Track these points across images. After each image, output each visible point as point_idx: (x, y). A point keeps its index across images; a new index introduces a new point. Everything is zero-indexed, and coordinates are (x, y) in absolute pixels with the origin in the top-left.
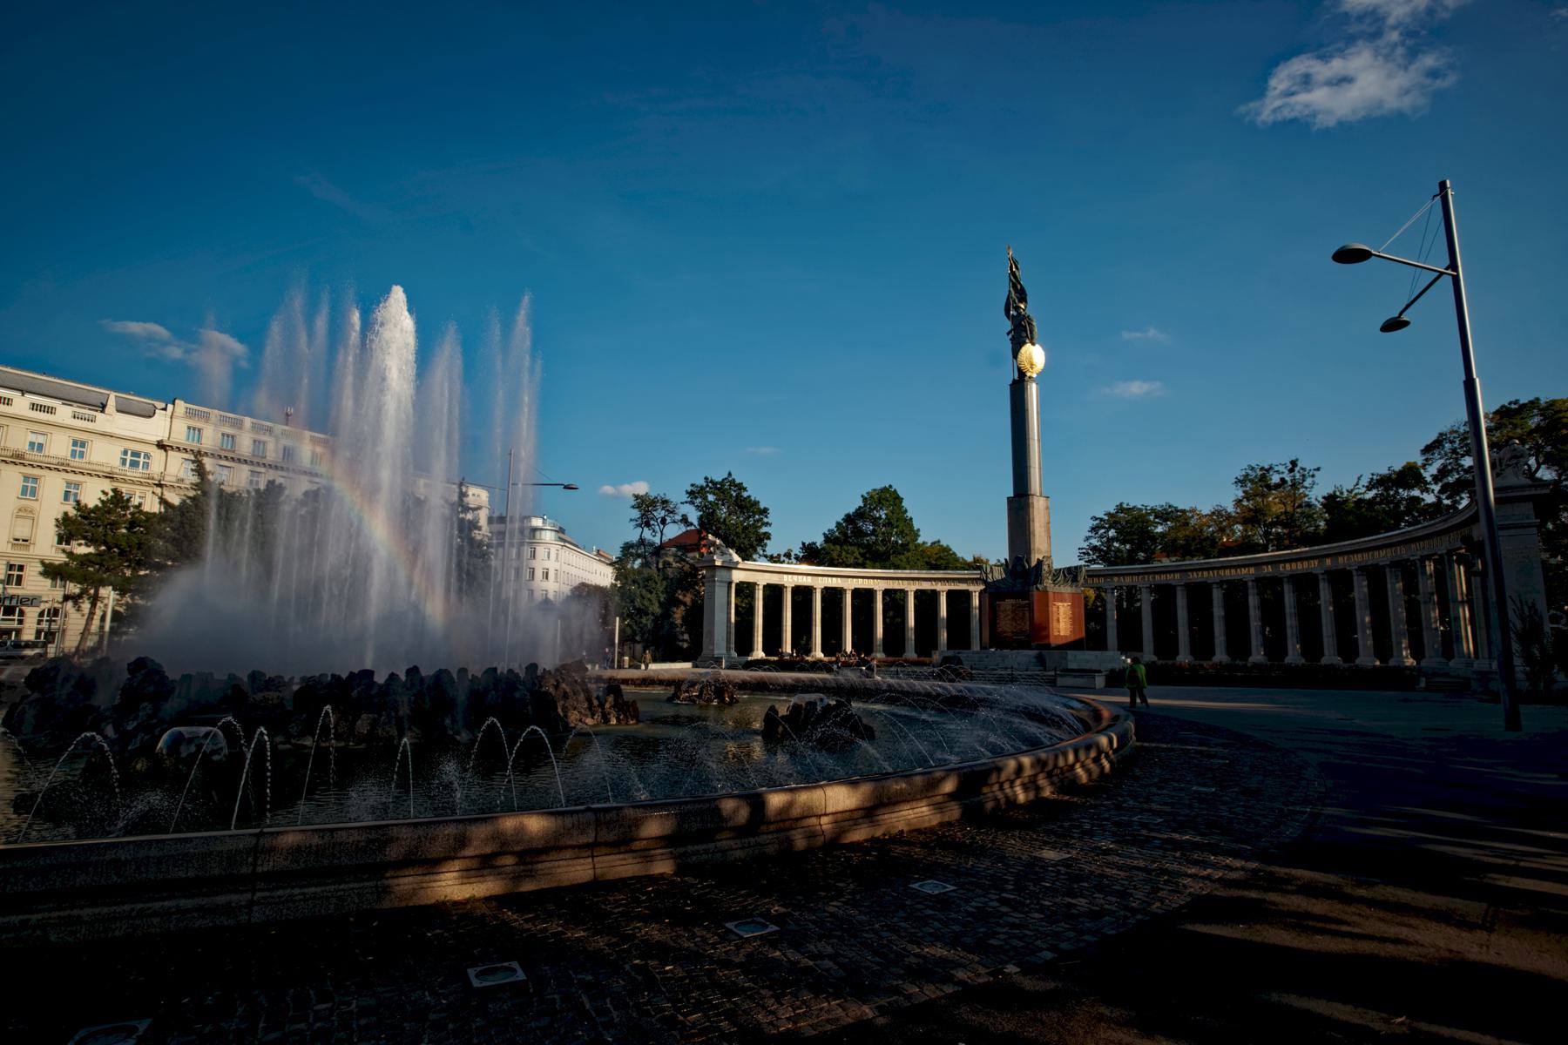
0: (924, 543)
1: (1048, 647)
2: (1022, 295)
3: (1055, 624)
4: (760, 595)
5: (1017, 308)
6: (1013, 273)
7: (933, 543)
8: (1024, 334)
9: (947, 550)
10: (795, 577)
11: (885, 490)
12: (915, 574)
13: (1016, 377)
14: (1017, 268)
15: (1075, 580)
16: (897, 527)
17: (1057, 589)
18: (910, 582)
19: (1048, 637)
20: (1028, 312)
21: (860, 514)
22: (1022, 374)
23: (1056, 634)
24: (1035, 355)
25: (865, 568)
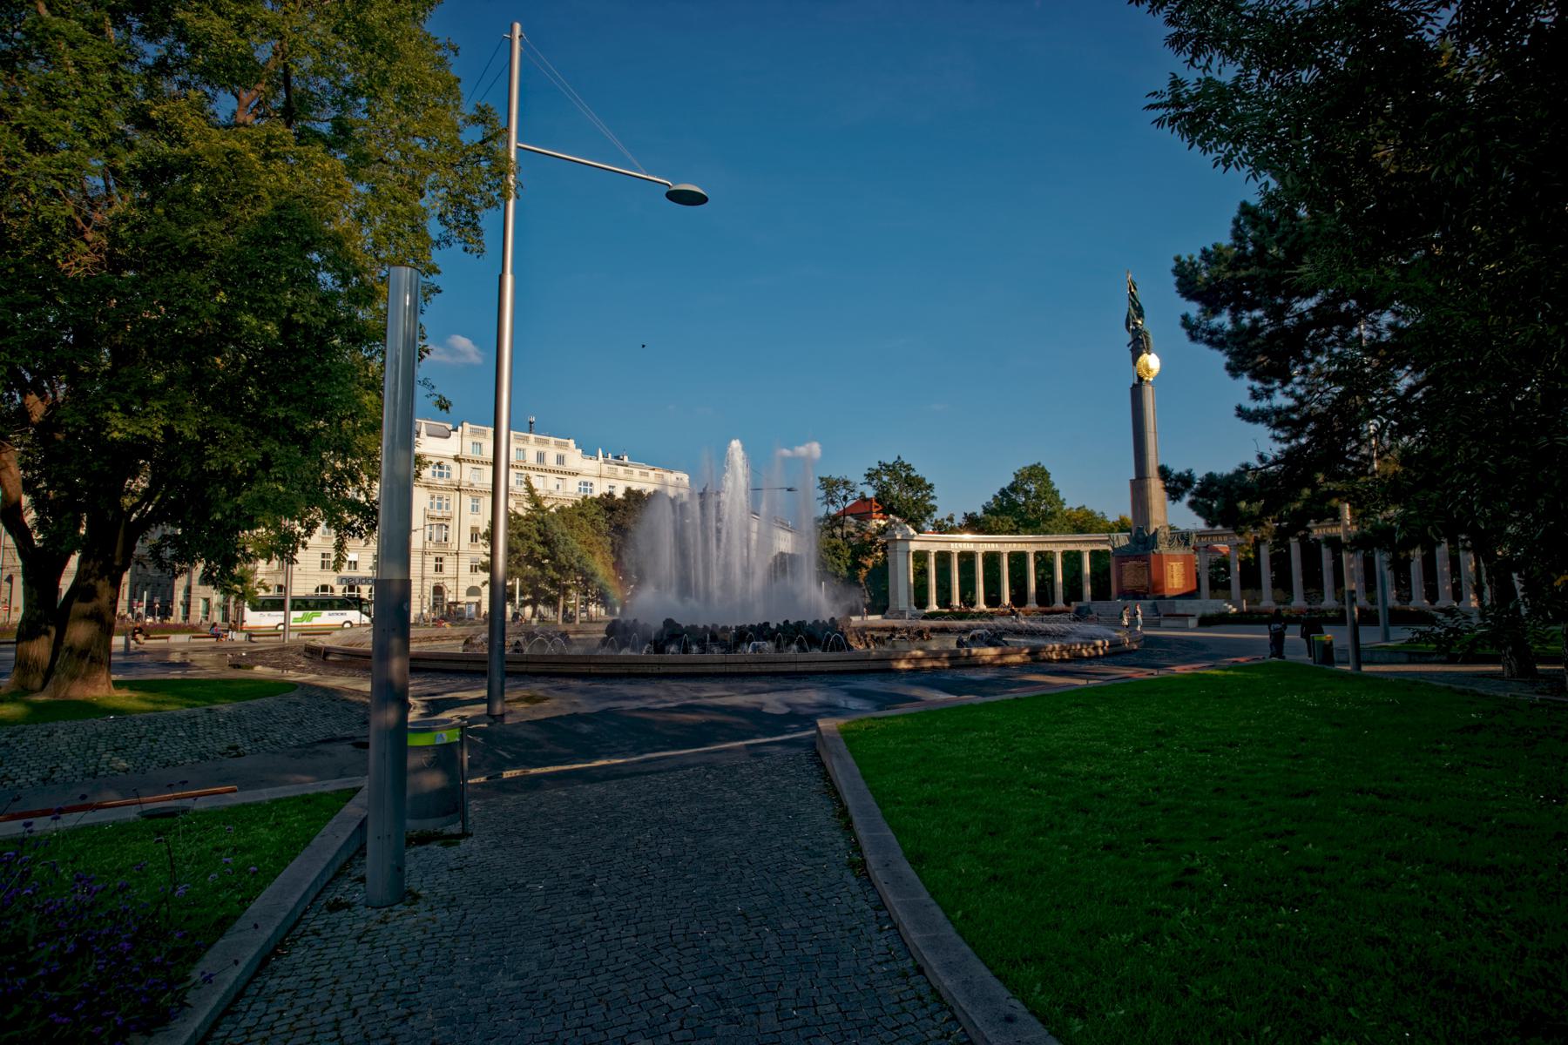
0: (1071, 509)
1: (1163, 597)
2: (1140, 313)
3: (1169, 579)
4: (932, 560)
5: (1135, 324)
6: (1132, 293)
7: (1079, 509)
8: (1141, 346)
9: (1090, 514)
10: (960, 545)
11: (1034, 467)
12: (1062, 538)
13: (1136, 382)
14: (1135, 288)
15: (1187, 544)
16: (1045, 498)
17: (1171, 552)
18: (1058, 545)
19: (1163, 590)
20: (1146, 328)
21: (1013, 488)
22: (1140, 379)
23: (1170, 586)
24: (1152, 362)
25: (1019, 534)
